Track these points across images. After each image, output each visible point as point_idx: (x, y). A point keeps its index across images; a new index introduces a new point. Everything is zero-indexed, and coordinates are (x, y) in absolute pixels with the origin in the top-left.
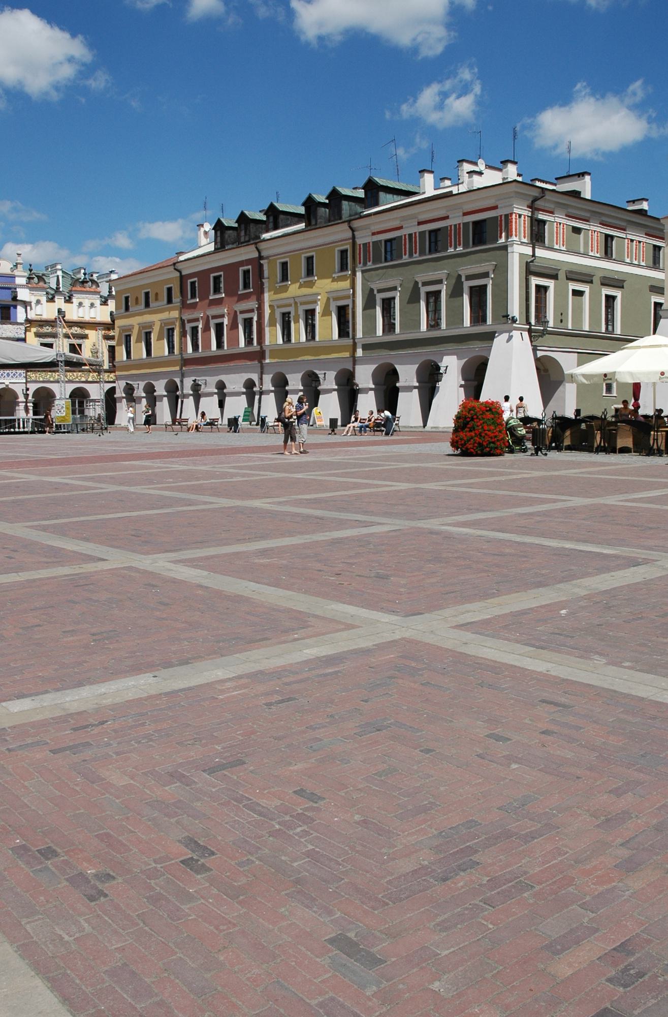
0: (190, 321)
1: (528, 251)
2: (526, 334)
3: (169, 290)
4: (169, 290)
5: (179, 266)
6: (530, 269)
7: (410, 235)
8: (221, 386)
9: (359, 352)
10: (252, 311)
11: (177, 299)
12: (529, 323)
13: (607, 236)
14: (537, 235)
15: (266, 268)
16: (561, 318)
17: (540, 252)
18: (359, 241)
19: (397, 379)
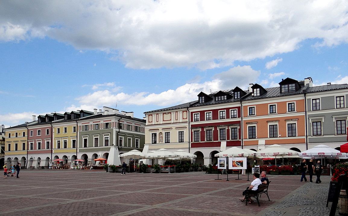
0: (30, 141)
1: (118, 130)
2: (117, 148)
3: (24, 133)
4: (24, 133)
5: (27, 127)
6: (118, 134)
7: (91, 125)
8: (39, 158)
9: (78, 151)
10: (49, 140)
11: (26, 135)
12: (118, 146)
13: (136, 127)
14: (120, 127)
15: (53, 129)
16: (125, 145)
17: (121, 130)
18: (78, 125)
19: (88, 158)
